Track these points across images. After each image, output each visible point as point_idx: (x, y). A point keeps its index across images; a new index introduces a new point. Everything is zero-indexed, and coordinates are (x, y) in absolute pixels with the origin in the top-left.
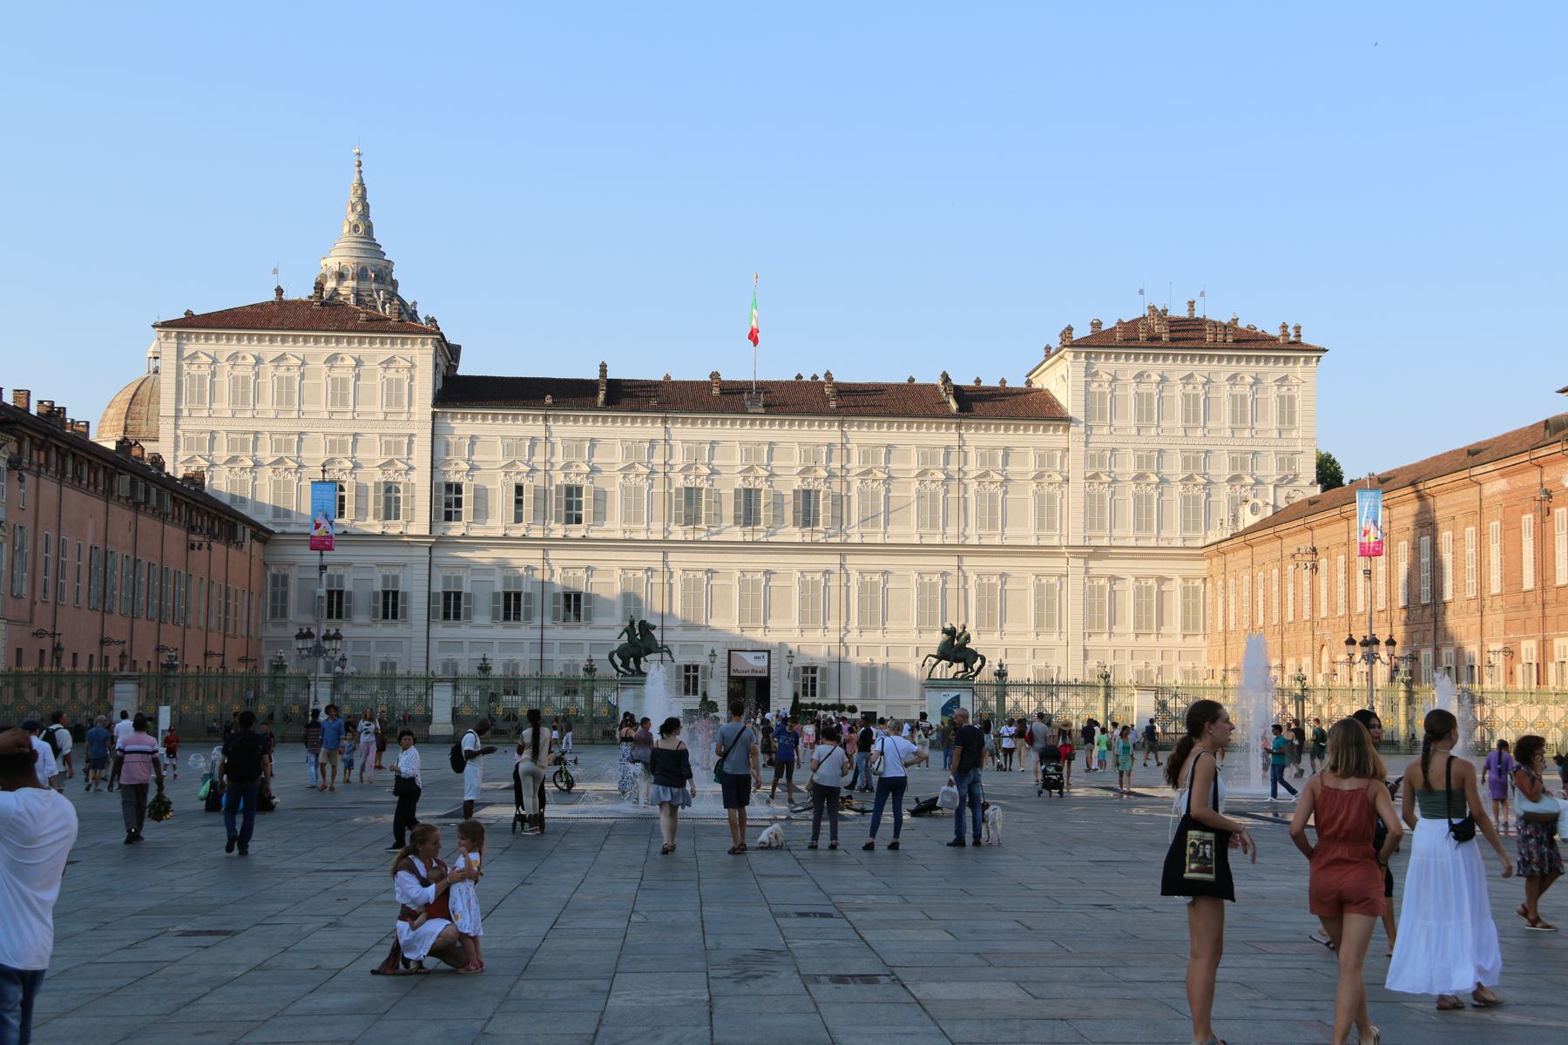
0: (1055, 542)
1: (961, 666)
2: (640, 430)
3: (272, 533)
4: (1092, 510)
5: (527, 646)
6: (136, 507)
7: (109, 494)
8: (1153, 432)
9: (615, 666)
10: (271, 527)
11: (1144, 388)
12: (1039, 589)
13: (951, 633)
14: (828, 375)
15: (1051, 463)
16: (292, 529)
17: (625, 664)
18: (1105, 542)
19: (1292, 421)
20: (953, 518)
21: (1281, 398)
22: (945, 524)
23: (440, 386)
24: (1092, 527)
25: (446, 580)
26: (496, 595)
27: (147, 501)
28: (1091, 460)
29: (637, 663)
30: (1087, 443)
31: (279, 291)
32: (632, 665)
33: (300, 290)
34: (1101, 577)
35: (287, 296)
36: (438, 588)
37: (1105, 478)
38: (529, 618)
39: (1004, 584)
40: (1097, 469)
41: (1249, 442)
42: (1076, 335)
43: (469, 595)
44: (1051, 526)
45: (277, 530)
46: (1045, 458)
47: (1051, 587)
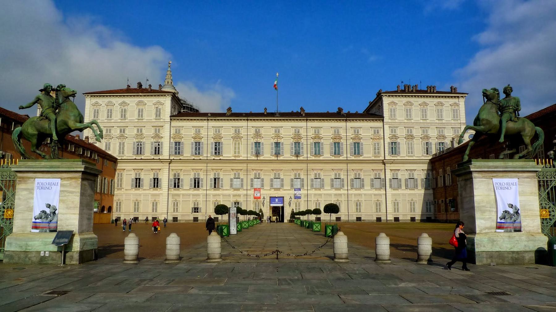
2: (242, 124)
3: (117, 159)
5: (201, 196)
10: (117, 157)
14: (301, 109)
16: (125, 158)
25: (175, 175)
26: (191, 179)
31: (129, 86)
33: (134, 86)
35: (132, 87)
36: (172, 177)
38: (202, 187)
42: (382, 92)
43: (182, 179)
45: (119, 158)
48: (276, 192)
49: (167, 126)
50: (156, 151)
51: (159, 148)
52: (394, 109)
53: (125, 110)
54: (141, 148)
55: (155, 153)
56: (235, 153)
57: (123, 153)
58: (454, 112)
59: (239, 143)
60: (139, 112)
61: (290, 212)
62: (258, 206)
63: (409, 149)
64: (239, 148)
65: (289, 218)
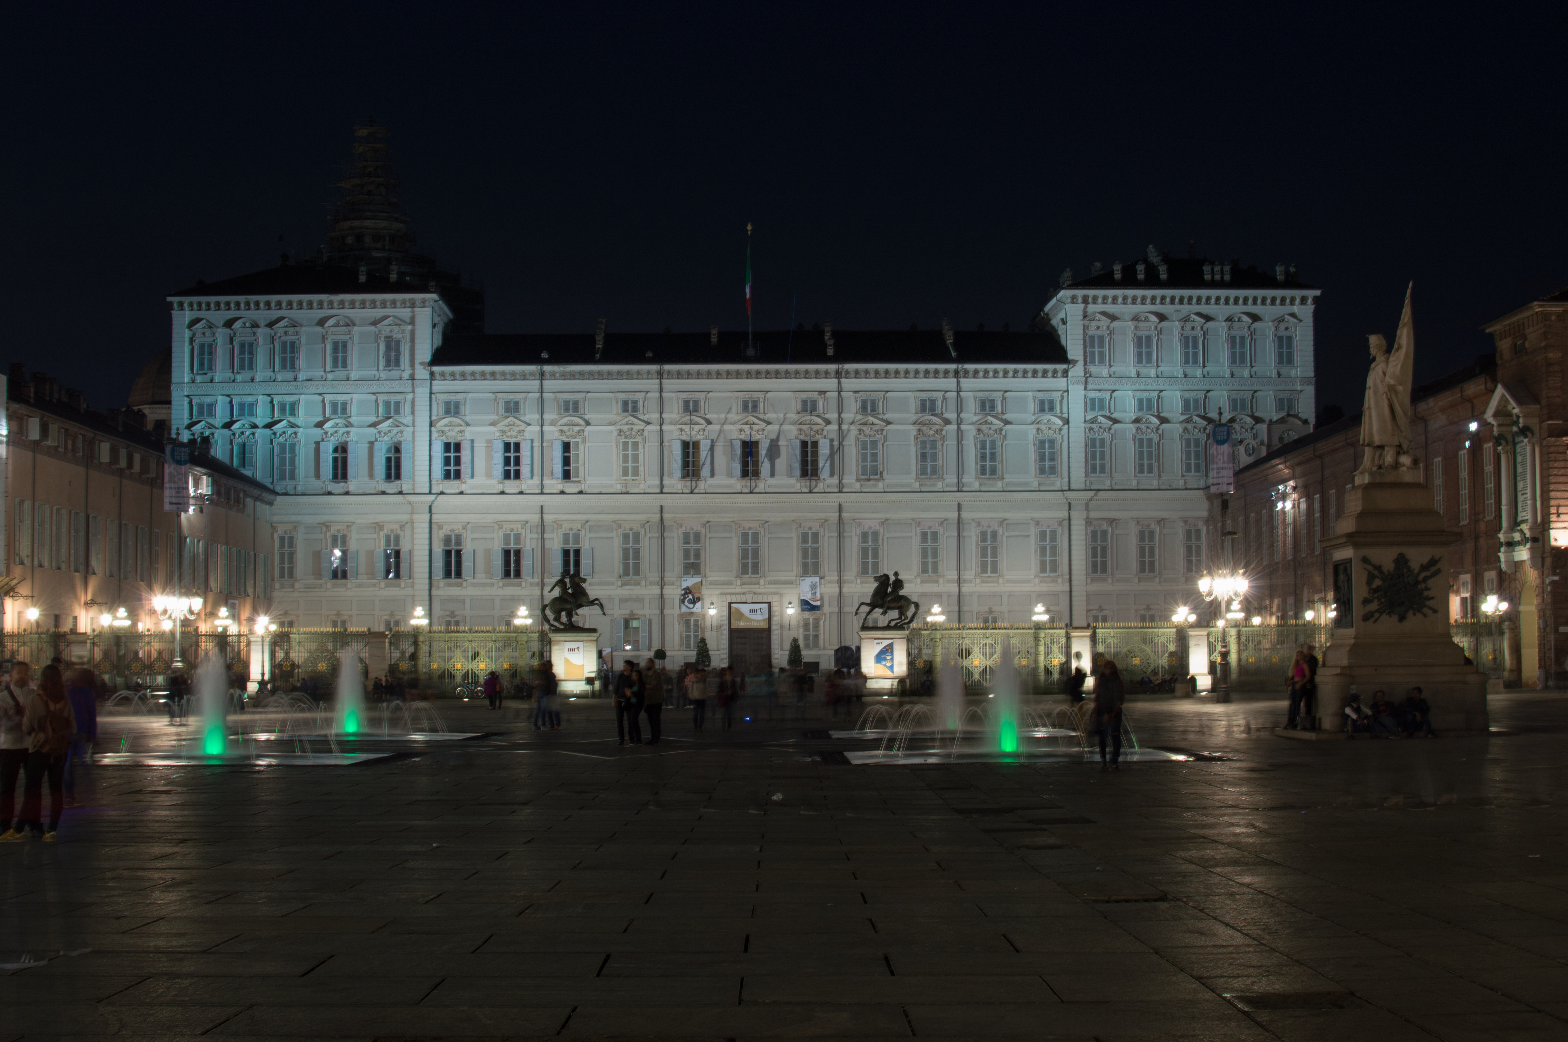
1: (894, 614)
4: (1094, 454)
6: (121, 473)
7: (89, 460)
9: (548, 621)
13: (883, 580)
17: (557, 619)
19: (1290, 361)
23: (438, 342)
25: (447, 540)
27: (130, 465)
29: (570, 615)
32: (564, 617)
48: (746, 588)
49: (422, 392)
50: (389, 468)
51: (398, 461)
52: (1101, 338)
53: (293, 344)
54: (345, 461)
55: (388, 477)
56: (625, 472)
57: (293, 477)
58: (1280, 346)
59: (636, 444)
60: (335, 350)
61: (787, 646)
62: (696, 631)
63: (1141, 458)
64: (636, 459)
65: (785, 664)
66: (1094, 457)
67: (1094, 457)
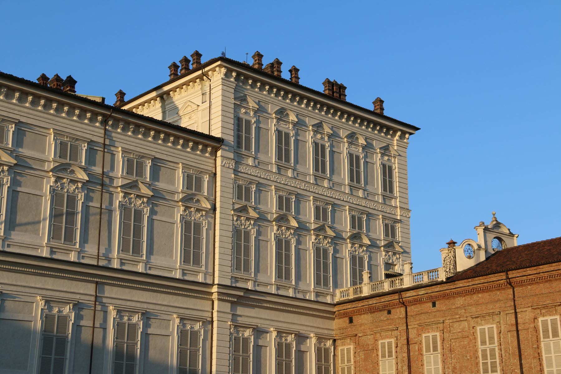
0: (200, 278)
4: (239, 246)
8: (290, 173)
11: (283, 127)
12: (182, 334)
15: (199, 187)
18: (250, 286)
19: (391, 191)
20: (93, 233)
21: (384, 166)
22: (84, 240)
24: (238, 268)
28: (241, 192)
30: (236, 171)
34: (246, 327)
37: (253, 214)
39: (146, 325)
40: (244, 202)
41: (363, 203)
44: (197, 262)
46: (193, 181)
47: (195, 335)
66: (238, 252)
67: (238, 252)
